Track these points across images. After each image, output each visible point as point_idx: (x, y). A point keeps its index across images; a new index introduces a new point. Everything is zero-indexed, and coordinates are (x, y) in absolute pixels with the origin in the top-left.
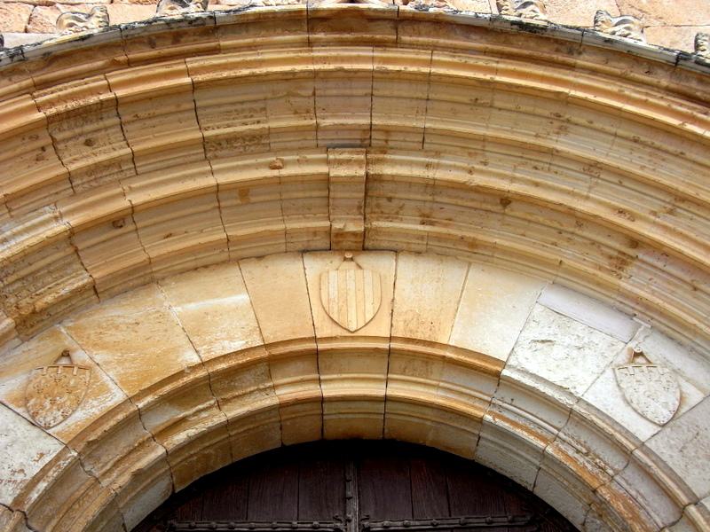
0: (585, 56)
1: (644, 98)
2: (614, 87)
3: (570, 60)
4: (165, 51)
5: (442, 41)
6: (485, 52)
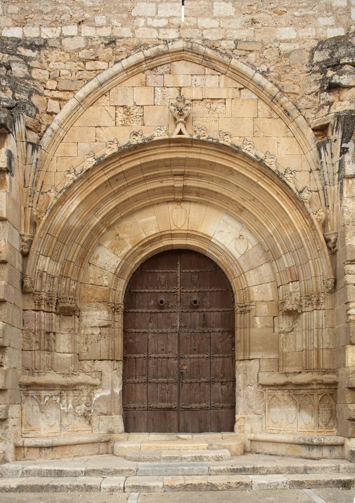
0: (239, 154)
1: (251, 170)
2: (244, 165)
3: (235, 156)
4: (133, 152)
5: (203, 147)
6: (214, 150)
